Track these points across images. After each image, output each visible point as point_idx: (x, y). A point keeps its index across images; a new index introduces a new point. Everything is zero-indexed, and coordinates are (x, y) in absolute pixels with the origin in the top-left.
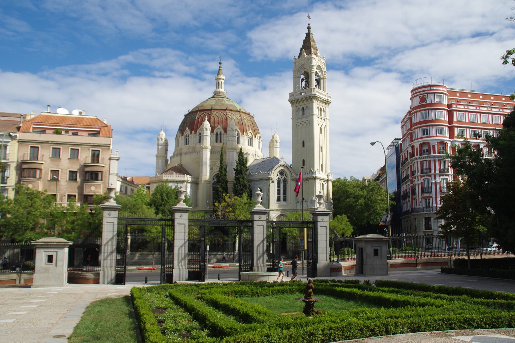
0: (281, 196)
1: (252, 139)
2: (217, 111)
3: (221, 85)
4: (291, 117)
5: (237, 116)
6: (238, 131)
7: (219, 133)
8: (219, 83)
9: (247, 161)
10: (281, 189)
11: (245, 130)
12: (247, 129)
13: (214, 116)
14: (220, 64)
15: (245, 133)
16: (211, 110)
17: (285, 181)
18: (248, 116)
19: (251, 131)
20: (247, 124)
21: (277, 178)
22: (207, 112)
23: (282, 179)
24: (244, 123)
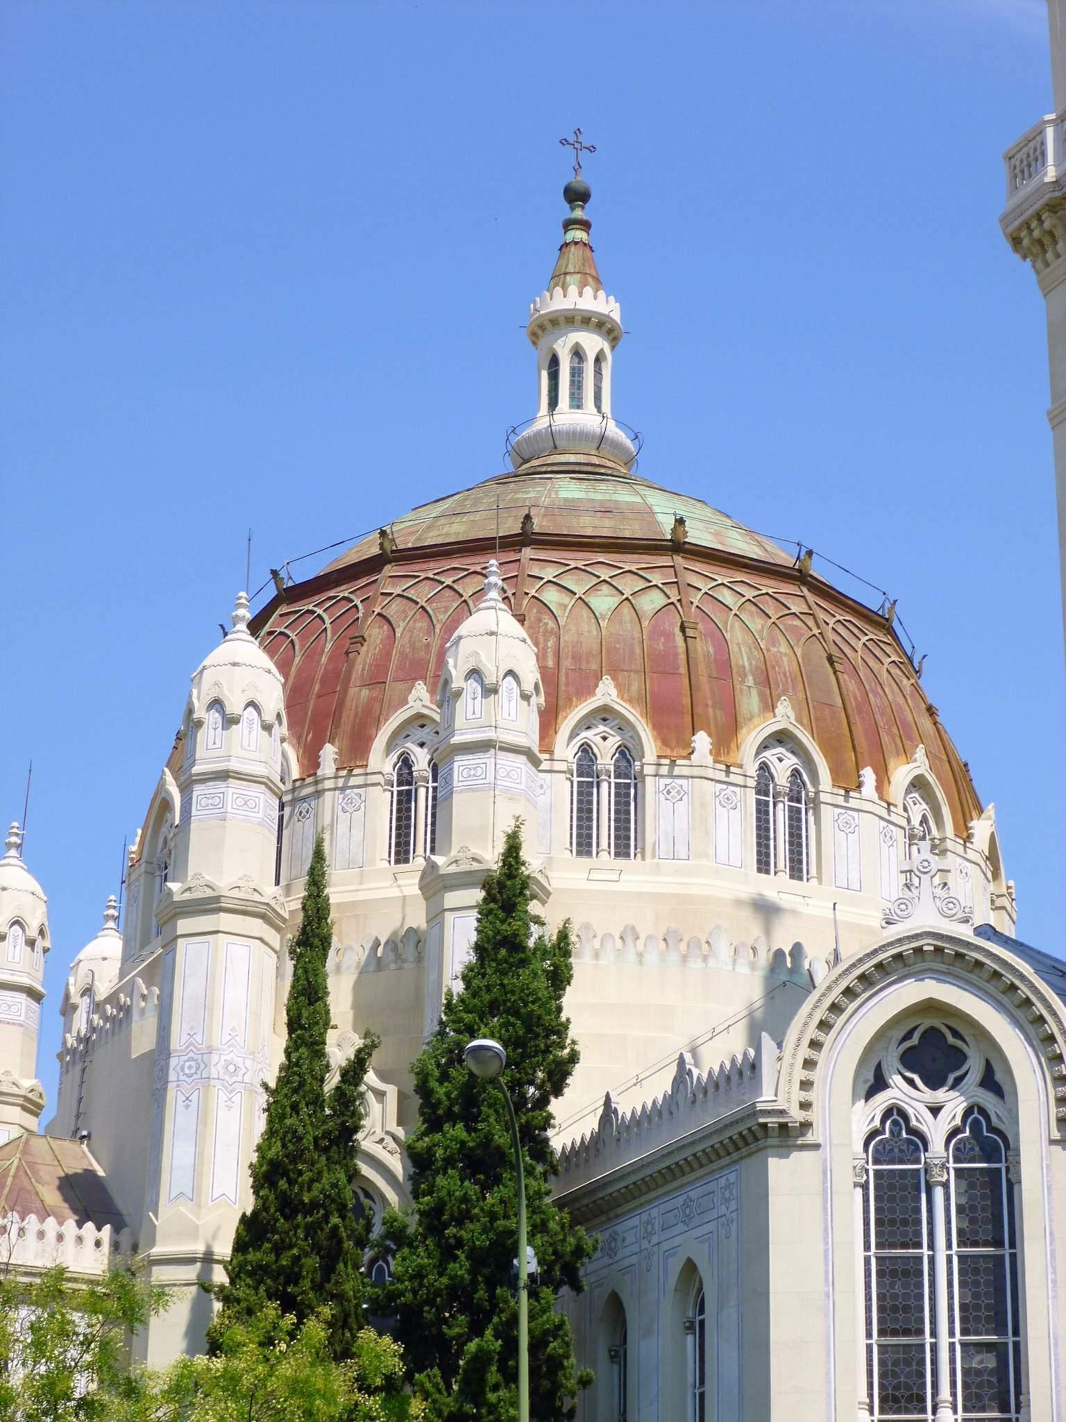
0: (944, 1338)
1: (799, 792)
2: (430, 569)
3: (576, 374)
4: (1048, 404)
5: (629, 585)
6: (623, 726)
7: (421, 760)
8: (554, 362)
9: (559, 979)
10: (942, 1254)
11: (714, 714)
12: (750, 701)
13: (393, 611)
14: (577, 196)
15: (702, 741)
16: (371, 566)
17: (988, 1142)
18: (769, 586)
19: (785, 716)
20: (743, 657)
21: (865, 1116)
22: (343, 591)
23: (936, 1131)
24: (703, 648)
